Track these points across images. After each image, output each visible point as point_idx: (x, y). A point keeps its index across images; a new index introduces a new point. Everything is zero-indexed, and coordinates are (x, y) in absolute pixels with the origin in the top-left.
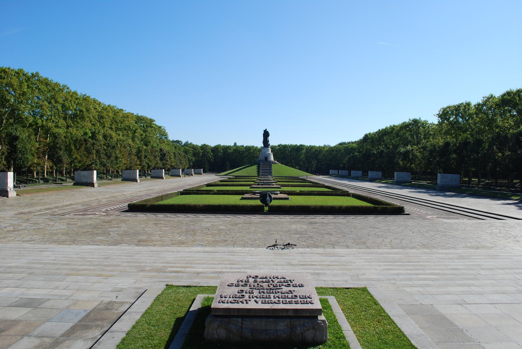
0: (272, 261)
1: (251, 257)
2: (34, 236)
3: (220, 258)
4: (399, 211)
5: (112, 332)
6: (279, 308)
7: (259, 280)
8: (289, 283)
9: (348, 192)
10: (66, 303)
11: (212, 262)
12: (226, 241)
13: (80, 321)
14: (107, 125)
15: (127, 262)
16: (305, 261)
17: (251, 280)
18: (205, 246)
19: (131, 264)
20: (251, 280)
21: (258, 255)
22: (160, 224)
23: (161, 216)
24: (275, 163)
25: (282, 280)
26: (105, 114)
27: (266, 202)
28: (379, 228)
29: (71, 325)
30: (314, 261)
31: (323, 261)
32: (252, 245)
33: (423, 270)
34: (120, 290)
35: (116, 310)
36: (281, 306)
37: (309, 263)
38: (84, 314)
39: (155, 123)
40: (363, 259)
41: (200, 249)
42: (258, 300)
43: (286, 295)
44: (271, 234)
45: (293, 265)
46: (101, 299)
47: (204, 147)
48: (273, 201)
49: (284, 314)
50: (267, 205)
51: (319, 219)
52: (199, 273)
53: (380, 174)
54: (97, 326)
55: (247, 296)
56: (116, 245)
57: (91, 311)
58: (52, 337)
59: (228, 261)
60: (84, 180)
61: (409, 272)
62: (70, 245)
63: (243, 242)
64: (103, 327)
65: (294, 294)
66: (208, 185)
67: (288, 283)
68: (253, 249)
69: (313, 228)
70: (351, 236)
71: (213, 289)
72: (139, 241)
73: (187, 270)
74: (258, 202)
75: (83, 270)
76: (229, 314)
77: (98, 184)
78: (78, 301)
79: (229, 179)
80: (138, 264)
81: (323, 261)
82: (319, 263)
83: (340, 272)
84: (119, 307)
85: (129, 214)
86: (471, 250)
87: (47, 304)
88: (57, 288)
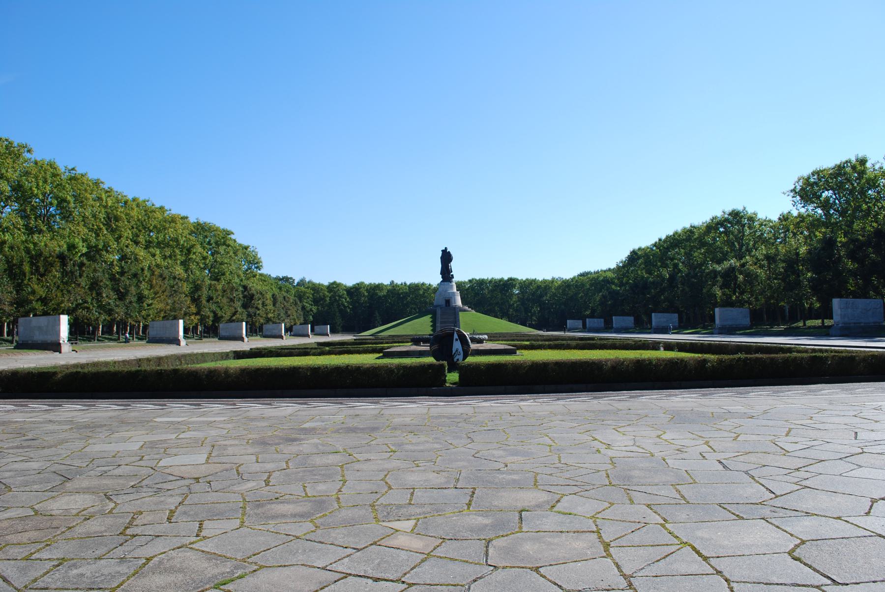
14: (127, 233)
24: (465, 311)
26: (120, 211)
39: (233, 237)
47: (333, 287)
50: (453, 367)
60: (38, 337)
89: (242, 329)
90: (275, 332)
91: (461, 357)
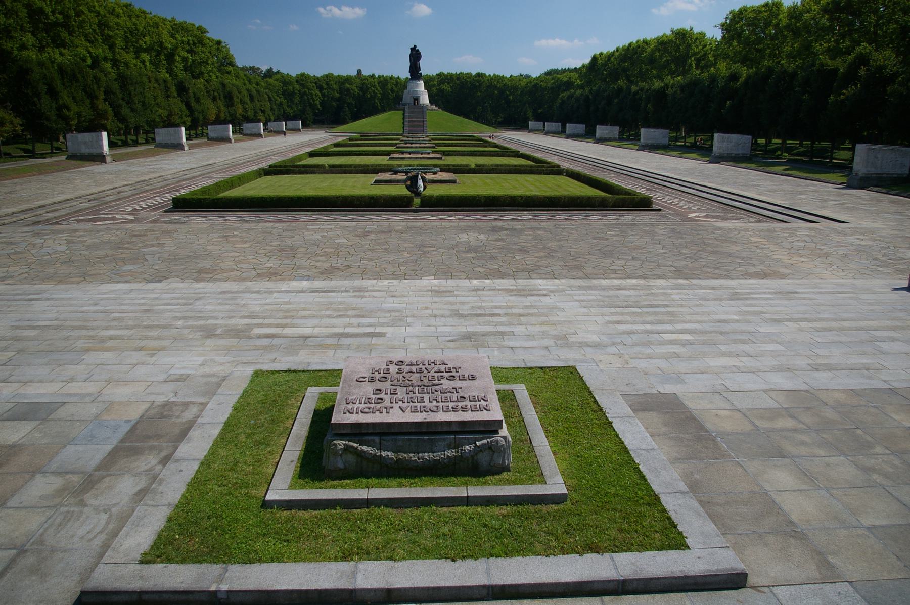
0: (426, 308)
1: (392, 300)
2: (11, 269)
3: (341, 303)
4: (643, 204)
5: (177, 461)
6: (437, 420)
7: (406, 368)
8: (453, 374)
9: (558, 166)
10: (94, 410)
11: (328, 313)
12: (349, 267)
13: (122, 441)
14: (119, 42)
15: (184, 318)
16: (480, 308)
17: (393, 369)
18: (314, 279)
19: (190, 323)
20: (393, 369)
21: (403, 296)
22: (234, 236)
23: (232, 219)
24: (432, 110)
25: (443, 368)
26: (112, 20)
27: (417, 189)
28: (607, 239)
29: (109, 447)
30: (496, 307)
31: (511, 307)
32: (394, 276)
33: (670, 322)
34: (182, 379)
35: (178, 417)
36: (441, 417)
37: (488, 312)
38: (126, 428)
39: (208, 35)
40: (577, 301)
41: (305, 284)
42: (404, 406)
43: (449, 395)
44: (424, 252)
45: (462, 316)
46: (152, 398)
47: (303, 79)
48: (428, 186)
49: (445, 429)
51: (508, 219)
52: (306, 337)
53: (616, 130)
54: (152, 448)
55: (387, 398)
56: (160, 281)
57: (137, 423)
58: (82, 472)
59: (354, 309)
60: (85, 150)
61: (648, 327)
62: (78, 283)
63: (378, 270)
64: (161, 451)
65: (461, 394)
66: (312, 154)
67: (452, 373)
68: (395, 282)
69: (497, 240)
70: (559, 255)
71: (333, 376)
72: (200, 272)
73: (287, 331)
74: (401, 190)
75: (111, 338)
76: (358, 431)
77: (112, 155)
78: (112, 403)
79: (351, 139)
80: (202, 322)
81: (511, 307)
82: (504, 311)
83: (538, 329)
84: (182, 412)
85: (176, 216)
86: (753, 281)
87: (62, 413)
88: (72, 380)
89: (228, 131)
90: (255, 131)
91: (422, 189)
